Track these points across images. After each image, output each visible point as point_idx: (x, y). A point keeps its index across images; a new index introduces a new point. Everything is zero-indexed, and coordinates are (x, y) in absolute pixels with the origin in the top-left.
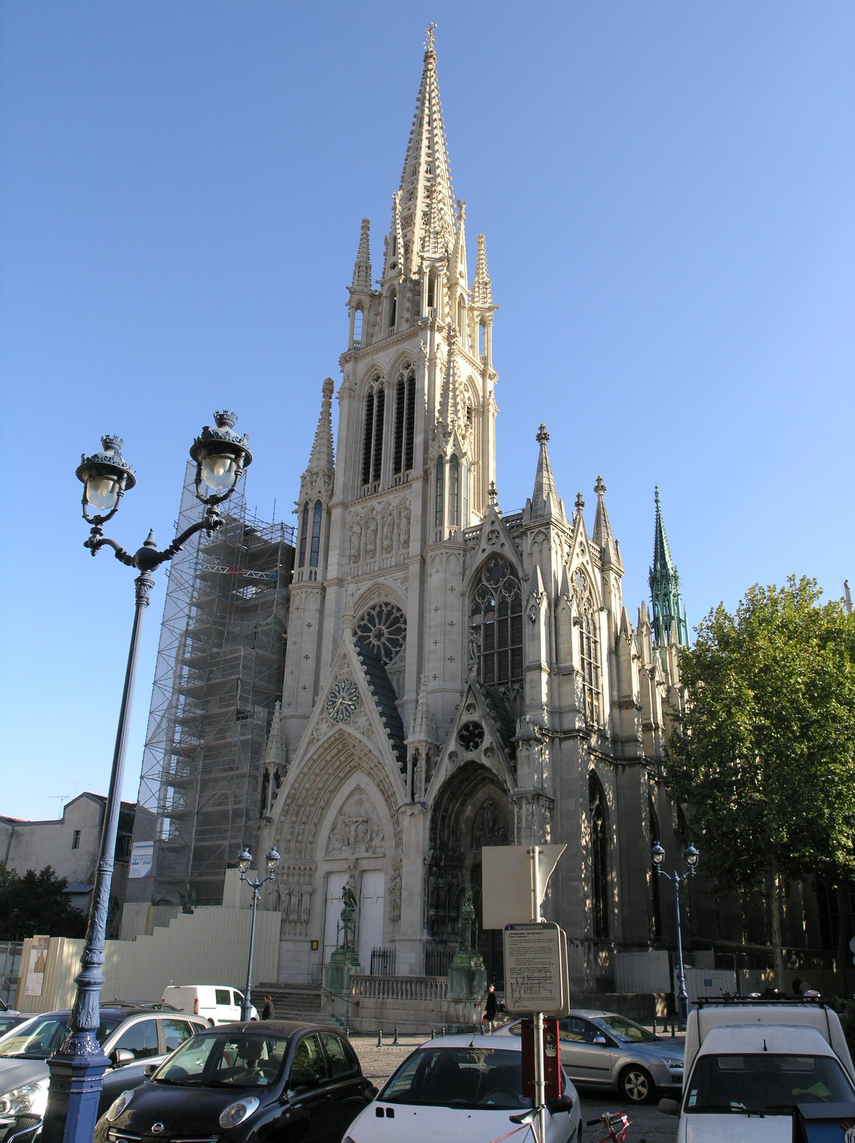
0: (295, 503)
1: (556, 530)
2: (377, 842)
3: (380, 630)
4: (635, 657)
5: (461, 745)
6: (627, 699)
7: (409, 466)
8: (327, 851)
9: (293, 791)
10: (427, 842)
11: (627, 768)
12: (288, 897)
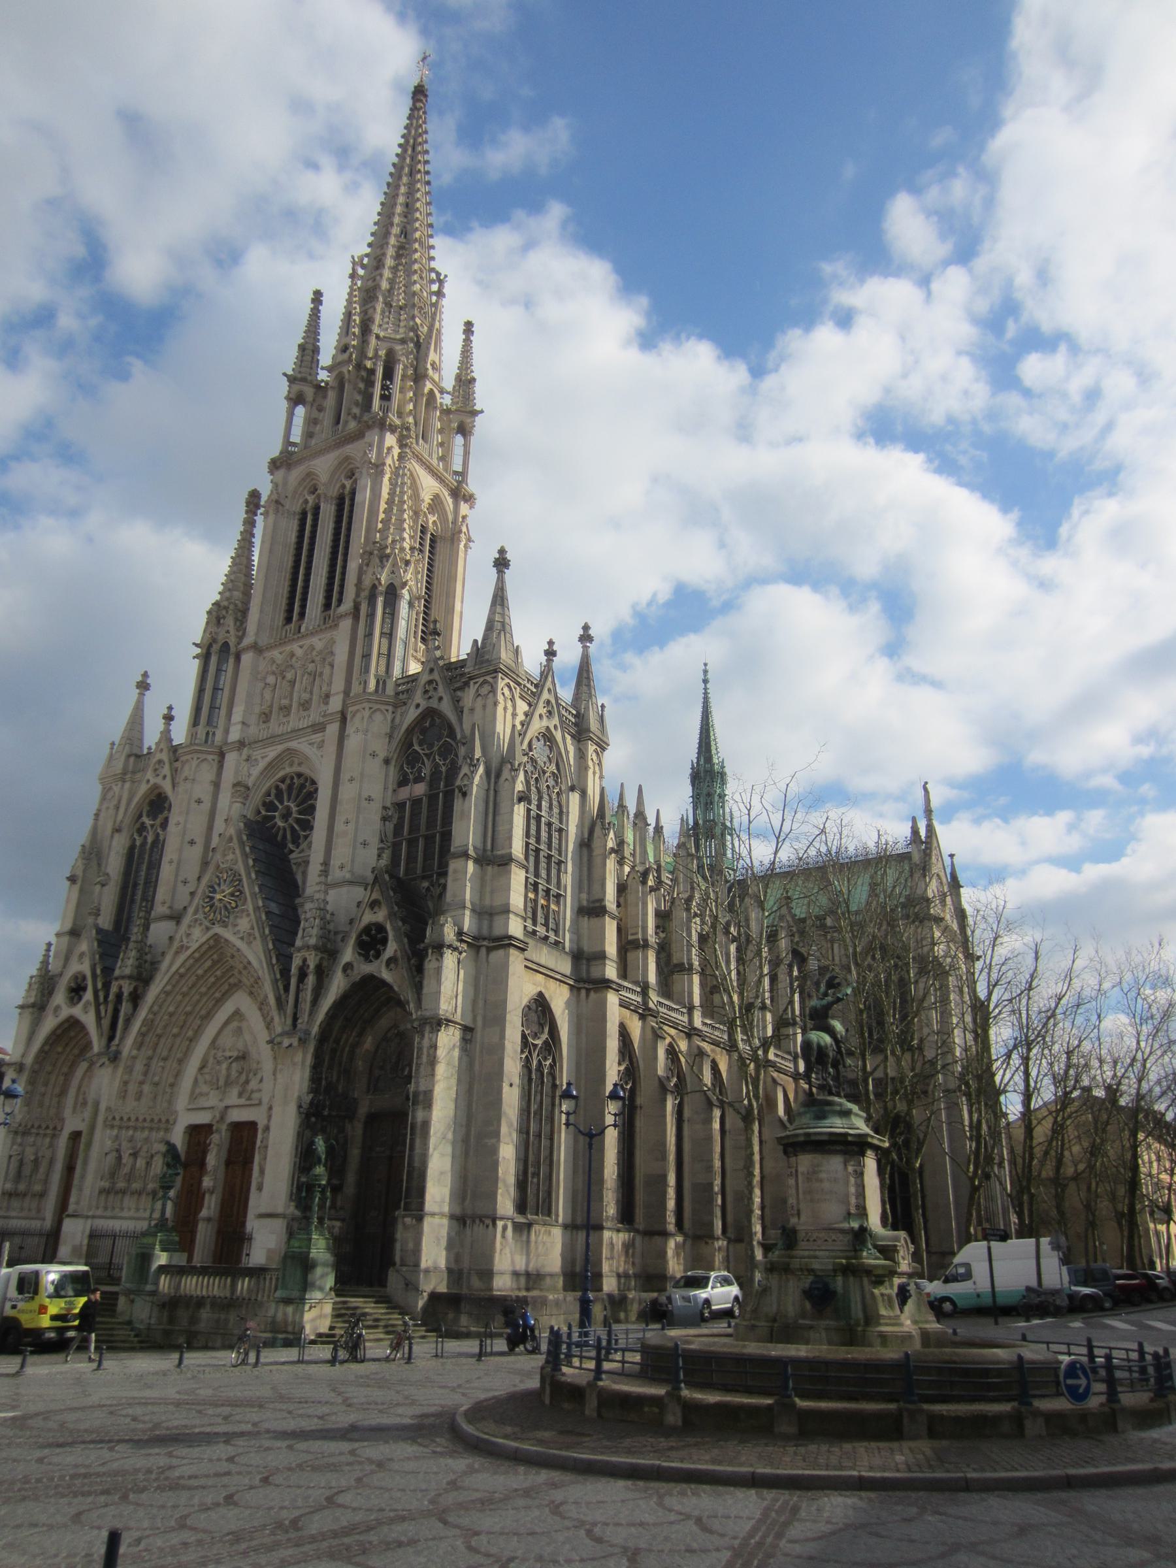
0: (196, 645)
1: (507, 680)
2: (253, 1084)
3: (288, 808)
4: (613, 850)
5: (360, 954)
6: (597, 904)
7: (340, 601)
8: (193, 1096)
9: (151, 1016)
10: (306, 1084)
11: (592, 994)
12: (131, 1160)
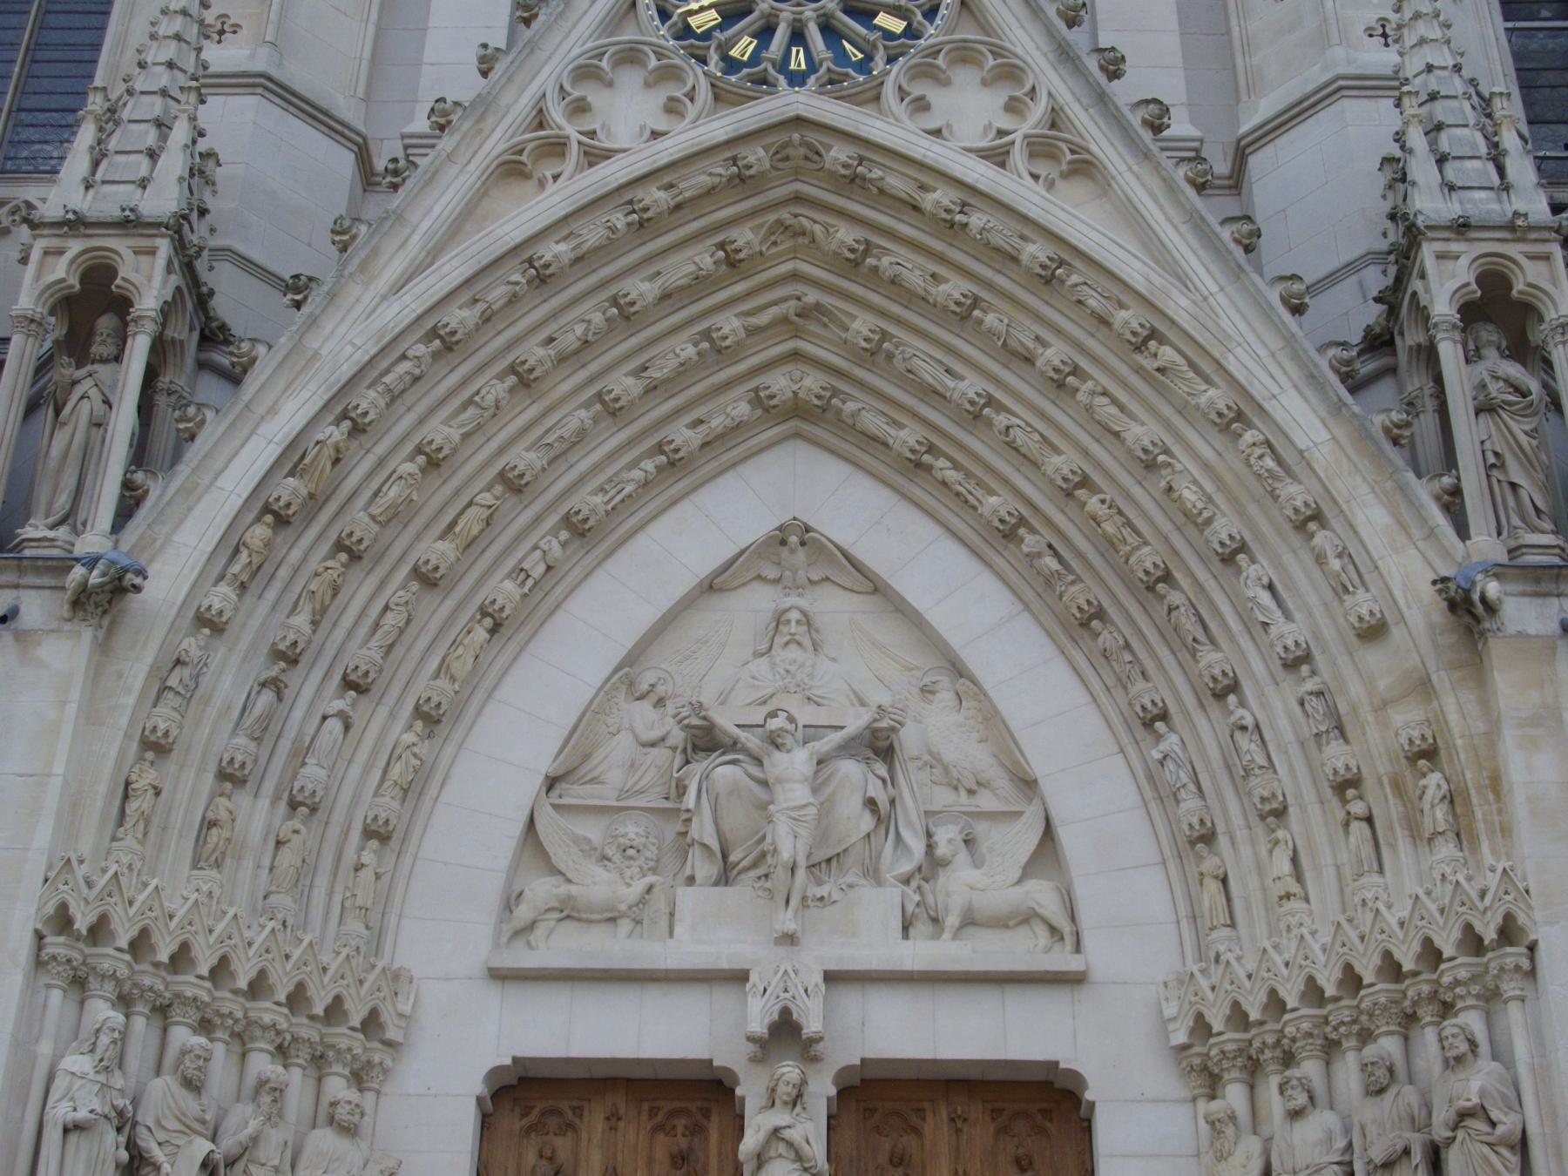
9: (335, 434)
